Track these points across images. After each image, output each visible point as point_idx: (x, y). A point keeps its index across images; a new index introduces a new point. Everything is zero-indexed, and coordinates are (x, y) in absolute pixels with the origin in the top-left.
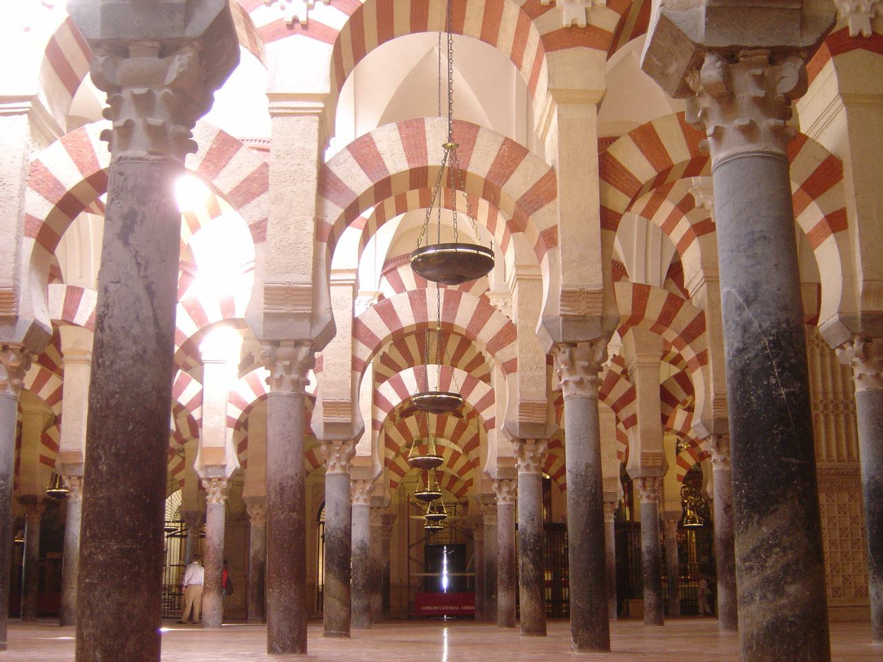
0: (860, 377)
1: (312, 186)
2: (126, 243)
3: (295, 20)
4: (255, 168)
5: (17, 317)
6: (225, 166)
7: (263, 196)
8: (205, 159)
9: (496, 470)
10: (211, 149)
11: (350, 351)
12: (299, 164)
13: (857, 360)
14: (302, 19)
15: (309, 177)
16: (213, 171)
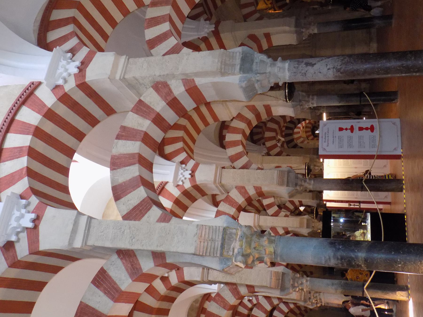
0: (313, 30)
1: (245, 171)
2: (315, 64)
3: (190, 174)
4: (237, 191)
5: (282, 273)
6: (235, 200)
7: (246, 188)
8: (232, 206)
9: (316, 201)
10: (228, 205)
11: (282, 218)
12: (238, 175)
13: (307, 31)
14: (190, 172)
15: (242, 172)
16: (236, 204)
